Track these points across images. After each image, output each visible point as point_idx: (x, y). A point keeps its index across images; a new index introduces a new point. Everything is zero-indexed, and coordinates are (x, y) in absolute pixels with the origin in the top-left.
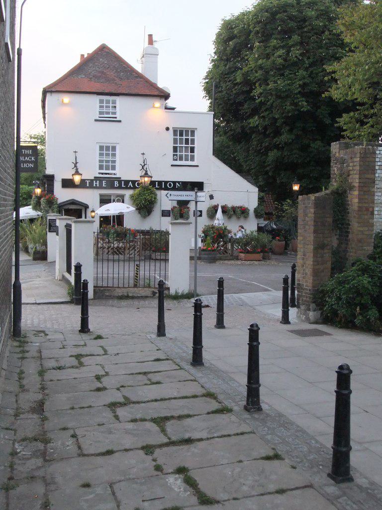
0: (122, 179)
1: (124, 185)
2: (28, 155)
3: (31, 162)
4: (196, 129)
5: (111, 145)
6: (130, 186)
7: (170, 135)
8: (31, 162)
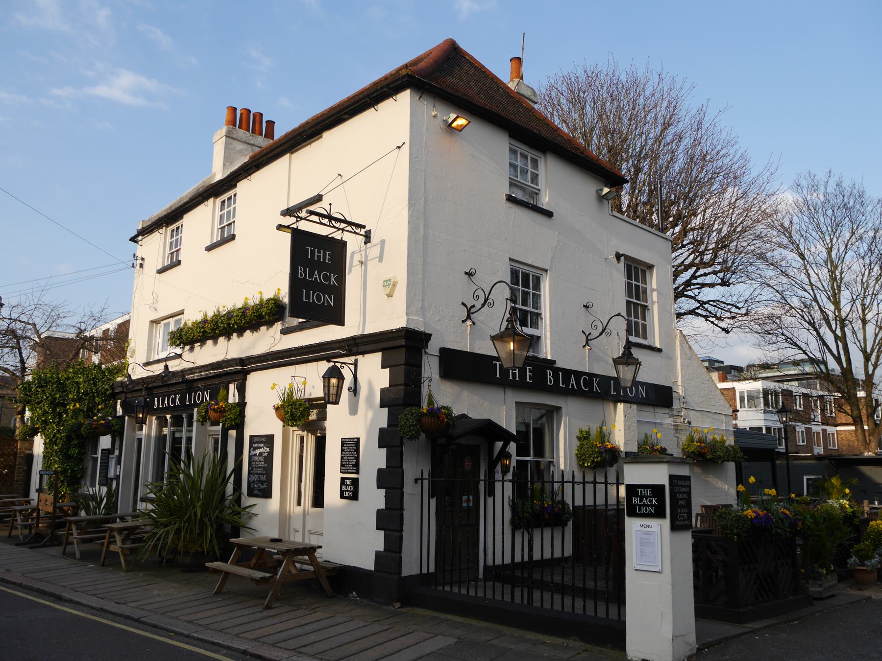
0: (559, 364)
1: (563, 385)
5: (532, 272)
6: (573, 384)
7: (619, 272)
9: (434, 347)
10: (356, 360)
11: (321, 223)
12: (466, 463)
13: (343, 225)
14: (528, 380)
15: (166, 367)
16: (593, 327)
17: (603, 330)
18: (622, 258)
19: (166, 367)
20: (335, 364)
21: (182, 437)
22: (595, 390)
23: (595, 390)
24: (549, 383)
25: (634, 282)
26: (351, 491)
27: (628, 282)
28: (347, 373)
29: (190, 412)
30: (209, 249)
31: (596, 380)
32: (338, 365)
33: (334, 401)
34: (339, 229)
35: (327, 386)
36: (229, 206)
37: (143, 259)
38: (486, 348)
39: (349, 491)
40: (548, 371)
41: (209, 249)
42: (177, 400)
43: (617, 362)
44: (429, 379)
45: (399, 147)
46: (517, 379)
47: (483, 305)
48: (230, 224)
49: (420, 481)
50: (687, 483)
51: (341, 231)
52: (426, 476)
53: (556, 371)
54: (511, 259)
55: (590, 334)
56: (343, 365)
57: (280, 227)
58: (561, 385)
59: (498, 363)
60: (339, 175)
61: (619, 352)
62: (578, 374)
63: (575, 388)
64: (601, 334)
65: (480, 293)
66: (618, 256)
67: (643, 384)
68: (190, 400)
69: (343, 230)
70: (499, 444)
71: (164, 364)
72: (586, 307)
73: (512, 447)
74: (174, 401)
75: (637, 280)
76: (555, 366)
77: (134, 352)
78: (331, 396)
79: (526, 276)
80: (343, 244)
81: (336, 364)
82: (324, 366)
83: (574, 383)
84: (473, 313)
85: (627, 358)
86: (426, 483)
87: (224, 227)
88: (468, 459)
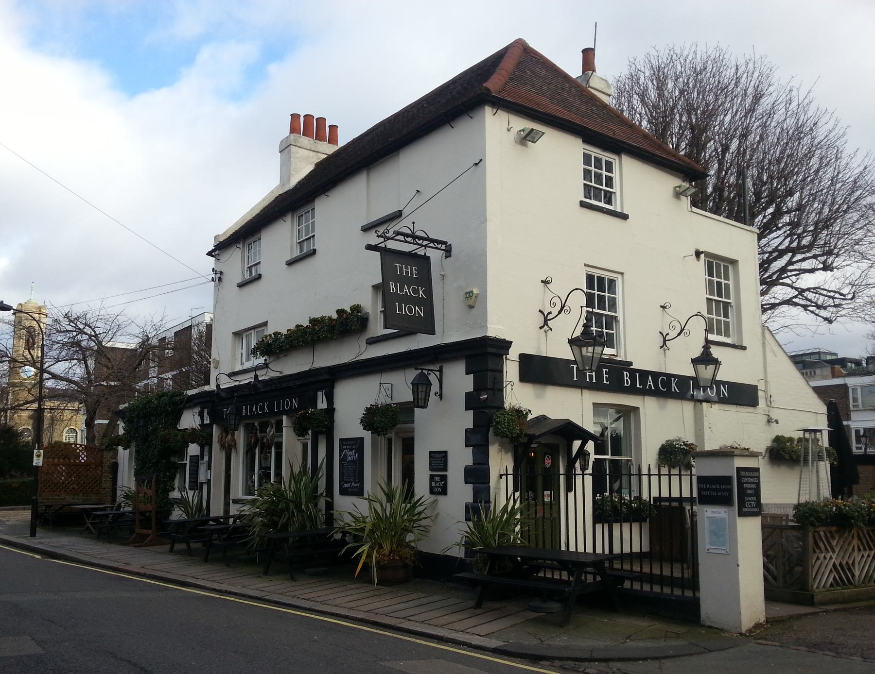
2: (408, 281)
3: (418, 302)
4: (734, 262)
5: (607, 275)
6: (650, 385)
8: (418, 302)
9: (514, 354)
10: (441, 368)
11: (406, 242)
12: (546, 461)
13: (425, 243)
14: (605, 382)
15: (256, 377)
16: (671, 327)
17: (682, 331)
18: (702, 256)
19: (256, 377)
20: (422, 371)
21: (282, 442)
22: (673, 391)
23: (673, 391)
24: (626, 385)
25: (715, 279)
26: (440, 487)
27: (709, 279)
28: (433, 378)
29: (278, 418)
30: (290, 263)
31: (674, 380)
32: (425, 372)
33: (423, 405)
34: (422, 246)
35: (415, 392)
36: (307, 221)
37: (221, 273)
38: (566, 353)
39: (438, 487)
40: (625, 373)
41: (290, 263)
42: (266, 407)
43: (695, 362)
44: (512, 383)
45: (476, 164)
46: (594, 381)
47: (560, 312)
48: (310, 238)
49: (504, 477)
50: (755, 474)
51: (424, 248)
52: (510, 471)
53: (633, 372)
54: (585, 265)
55: (668, 334)
56: (429, 372)
57: (369, 247)
58: (638, 386)
59: (575, 366)
60: (418, 191)
61: (697, 352)
62: (655, 375)
63: (653, 388)
64: (679, 334)
65: (556, 300)
66: (698, 254)
67: (724, 383)
68: (278, 408)
69: (426, 246)
70: (577, 444)
71: (252, 375)
72: (663, 307)
73: (590, 446)
74: (262, 408)
75: (719, 276)
76: (631, 367)
77: (217, 363)
78: (420, 401)
79: (601, 280)
80: (427, 259)
81: (424, 371)
82: (411, 374)
83: (652, 383)
84: (550, 320)
85: (705, 358)
86: (510, 478)
87: (303, 241)
88: (548, 457)
